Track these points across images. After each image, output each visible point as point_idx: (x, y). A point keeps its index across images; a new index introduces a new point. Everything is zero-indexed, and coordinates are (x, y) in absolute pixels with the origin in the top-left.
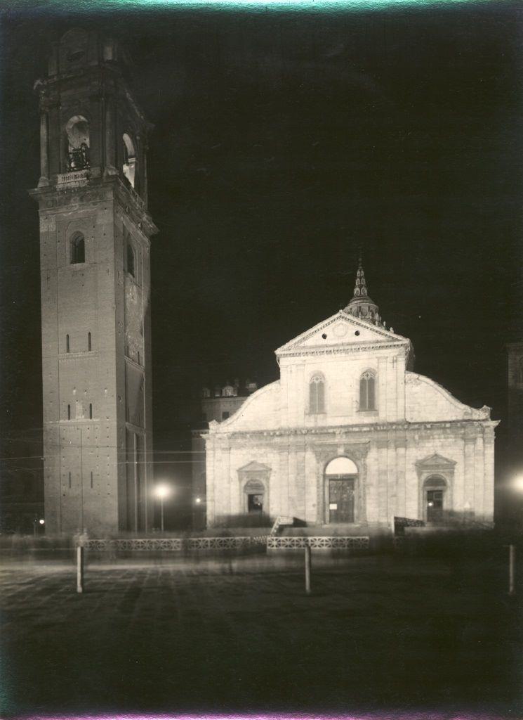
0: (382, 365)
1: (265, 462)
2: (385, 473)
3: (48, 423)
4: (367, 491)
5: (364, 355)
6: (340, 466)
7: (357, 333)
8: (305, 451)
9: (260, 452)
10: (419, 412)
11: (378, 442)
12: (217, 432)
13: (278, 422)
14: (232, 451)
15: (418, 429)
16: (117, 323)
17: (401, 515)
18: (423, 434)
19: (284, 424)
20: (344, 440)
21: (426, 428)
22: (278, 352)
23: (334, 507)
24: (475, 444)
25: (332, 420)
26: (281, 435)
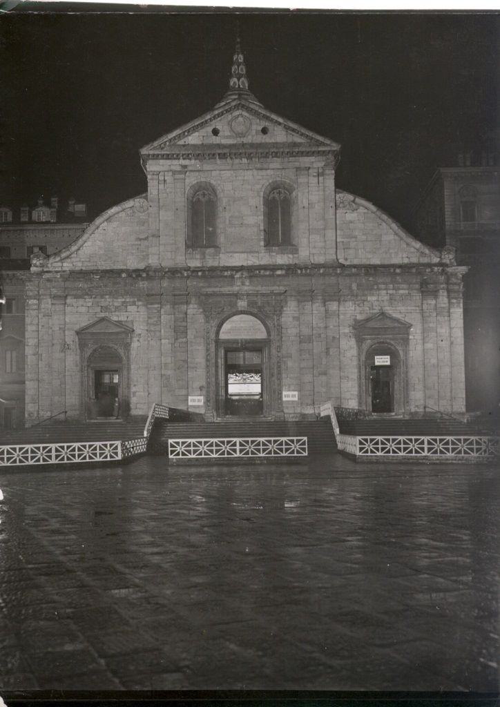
0: (302, 180)
1: (123, 318)
2: (309, 339)
5: (275, 163)
7: (264, 131)
8: (187, 303)
9: (116, 304)
10: (357, 250)
11: (299, 292)
14: (69, 301)
20: (246, 288)
22: (144, 151)
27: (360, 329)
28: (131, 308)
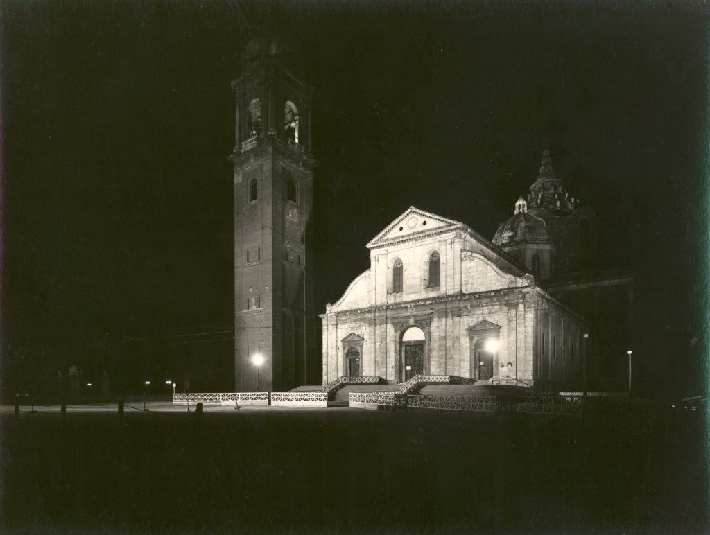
0: (443, 248)
2: (445, 338)
3: (237, 313)
4: (431, 355)
5: (429, 240)
6: (414, 334)
8: (386, 323)
10: (473, 284)
12: (331, 309)
13: (370, 301)
14: (339, 326)
15: (468, 299)
16: (274, 238)
17: (456, 374)
18: (474, 302)
19: (373, 302)
21: (476, 298)
22: (369, 246)
23: (409, 368)
24: (517, 309)
25: (407, 297)
26: (369, 312)
27: (472, 331)
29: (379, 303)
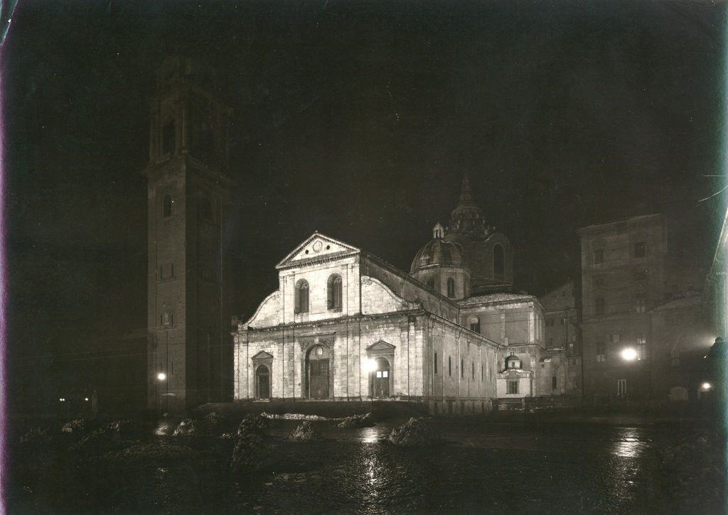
5: (332, 264)
8: (294, 341)
14: (250, 344)
19: (281, 321)
22: (278, 267)
24: (408, 330)
25: (313, 317)
28: (272, 346)
29: (287, 322)
